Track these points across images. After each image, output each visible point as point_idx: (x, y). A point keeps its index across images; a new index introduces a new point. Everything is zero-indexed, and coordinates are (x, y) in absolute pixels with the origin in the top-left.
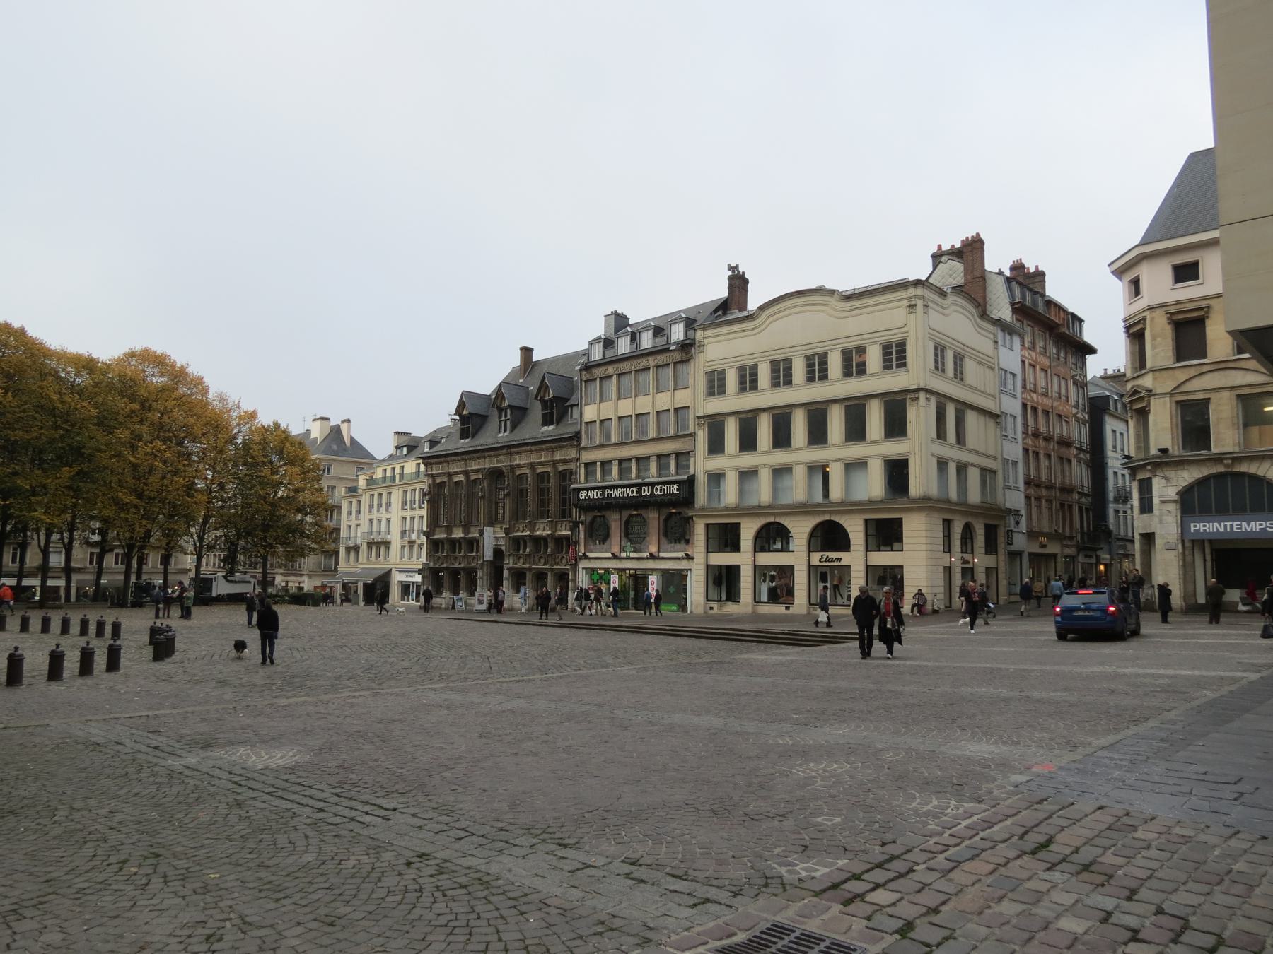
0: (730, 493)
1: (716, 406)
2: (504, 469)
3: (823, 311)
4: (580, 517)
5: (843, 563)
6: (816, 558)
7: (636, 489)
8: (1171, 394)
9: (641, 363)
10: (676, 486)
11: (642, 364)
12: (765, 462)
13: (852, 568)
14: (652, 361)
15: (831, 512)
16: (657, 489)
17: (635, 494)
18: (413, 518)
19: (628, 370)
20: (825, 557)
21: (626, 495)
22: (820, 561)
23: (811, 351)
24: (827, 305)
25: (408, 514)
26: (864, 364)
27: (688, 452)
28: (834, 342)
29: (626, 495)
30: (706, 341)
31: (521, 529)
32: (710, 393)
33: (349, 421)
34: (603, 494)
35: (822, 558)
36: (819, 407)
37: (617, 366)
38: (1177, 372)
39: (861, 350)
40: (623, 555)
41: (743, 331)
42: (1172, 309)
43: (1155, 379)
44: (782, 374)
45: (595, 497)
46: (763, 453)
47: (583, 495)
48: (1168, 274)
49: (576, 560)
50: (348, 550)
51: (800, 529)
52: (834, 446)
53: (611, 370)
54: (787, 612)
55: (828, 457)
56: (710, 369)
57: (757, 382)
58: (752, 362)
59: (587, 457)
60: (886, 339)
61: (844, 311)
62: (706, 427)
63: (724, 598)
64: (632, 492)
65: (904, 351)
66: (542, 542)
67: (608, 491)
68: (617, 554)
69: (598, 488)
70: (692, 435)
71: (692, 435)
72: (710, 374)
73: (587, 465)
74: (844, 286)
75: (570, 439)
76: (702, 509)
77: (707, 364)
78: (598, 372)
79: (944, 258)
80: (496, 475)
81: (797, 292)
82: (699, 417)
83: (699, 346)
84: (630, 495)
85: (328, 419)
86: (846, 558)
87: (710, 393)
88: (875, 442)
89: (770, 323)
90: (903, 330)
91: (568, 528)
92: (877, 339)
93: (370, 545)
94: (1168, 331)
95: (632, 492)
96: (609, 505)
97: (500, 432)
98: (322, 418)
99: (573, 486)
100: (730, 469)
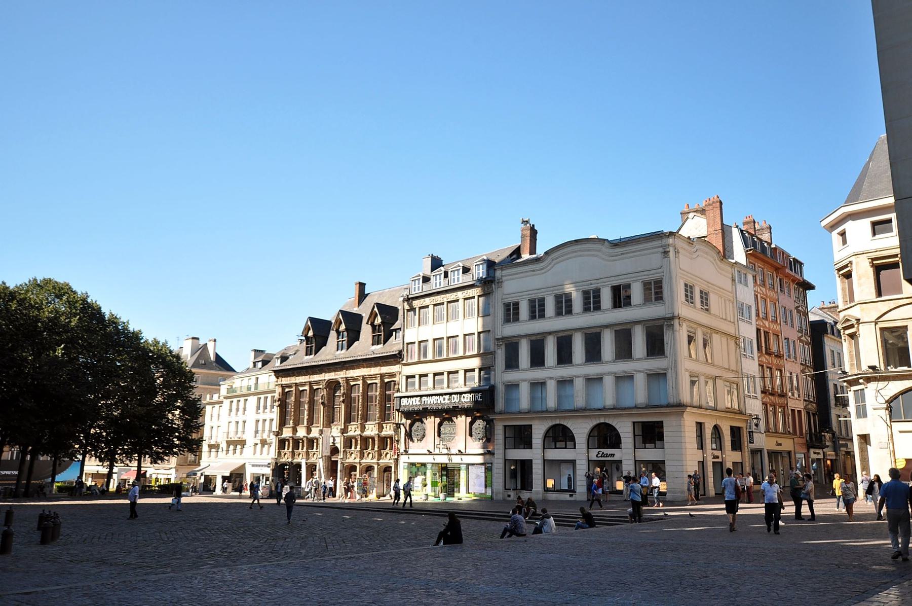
0: (524, 400)
2: (340, 380)
3: (596, 256)
4: (401, 420)
5: (615, 458)
6: (593, 454)
9: (451, 296)
10: (480, 395)
11: (452, 297)
12: (551, 375)
13: (624, 462)
14: (460, 295)
15: (605, 416)
17: (447, 401)
18: (265, 421)
19: (441, 302)
20: (601, 453)
21: (439, 402)
22: (597, 456)
23: (622, 281)
24: (599, 251)
25: (261, 417)
26: (629, 297)
27: (489, 367)
28: (605, 280)
29: (439, 402)
31: (353, 430)
33: (215, 340)
34: (420, 401)
35: (599, 454)
36: (594, 331)
39: (628, 287)
40: (437, 451)
41: (534, 271)
43: (862, 310)
44: (620, 298)
45: (414, 404)
46: (549, 368)
47: (404, 402)
49: (398, 455)
50: (211, 447)
51: (581, 429)
52: (606, 362)
53: (427, 301)
54: (572, 499)
55: (604, 371)
56: (506, 301)
57: (600, 303)
58: (540, 296)
59: (408, 371)
60: (647, 278)
62: (503, 347)
63: (519, 487)
64: (444, 399)
65: (661, 287)
66: (370, 440)
67: (424, 399)
68: (432, 450)
69: (417, 396)
72: (507, 306)
73: (408, 377)
74: (612, 236)
75: (394, 356)
76: (500, 413)
77: (504, 297)
78: (416, 304)
79: (691, 215)
80: (333, 386)
81: (575, 241)
82: (498, 339)
83: (498, 283)
84: (443, 402)
85: (198, 339)
86: (618, 454)
87: (507, 320)
88: (639, 359)
89: (555, 264)
90: (660, 270)
91: (392, 428)
92: (639, 278)
93: (229, 443)
95: (444, 399)
96: (425, 413)
97: (337, 350)
98: (193, 338)
99: (396, 395)
100: (523, 381)
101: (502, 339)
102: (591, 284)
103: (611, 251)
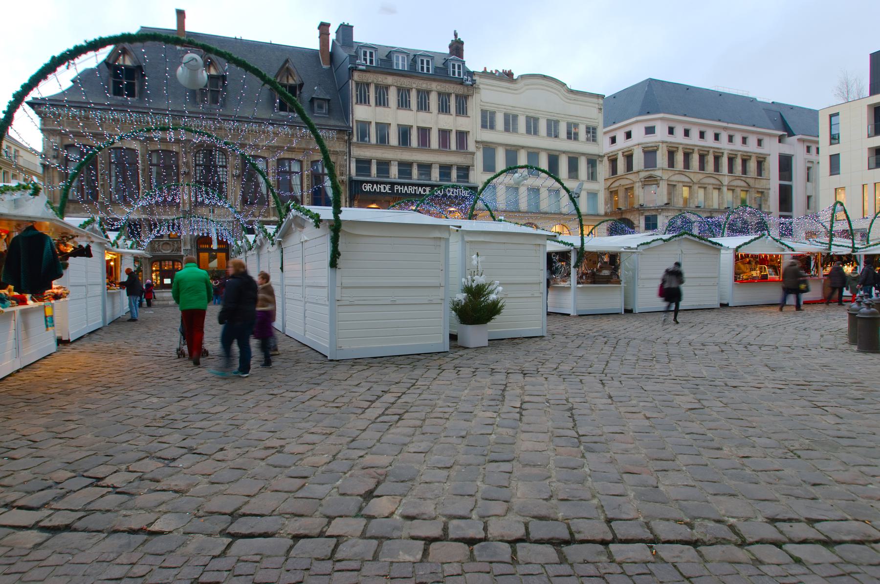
1: (488, 136)
7: (428, 189)
8: (668, 180)
16: (449, 191)
24: (559, 91)
29: (418, 193)
30: (481, 86)
32: (484, 126)
34: (392, 189)
37: (396, 78)
38: (700, 175)
41: (509, 89)
42: (644, 146)
43: (662, 173)
45: (382, 190)
48: (643, 131)
58: (515, 112)
61: (567, 99)
62: (481, 150)
64: (425, 191)
67: (396, 188)
70: (473, 154)
71: (473, 154)
72: (484, 113)
74: (572, 85)
77: (482, 103)
81: (544, 76)
82: (477, 142)
84: (422, 193)
94: (642, 155)
95: (425, 191)
101: (482, 142)
102: (554, 116)
103: (567, 94)
